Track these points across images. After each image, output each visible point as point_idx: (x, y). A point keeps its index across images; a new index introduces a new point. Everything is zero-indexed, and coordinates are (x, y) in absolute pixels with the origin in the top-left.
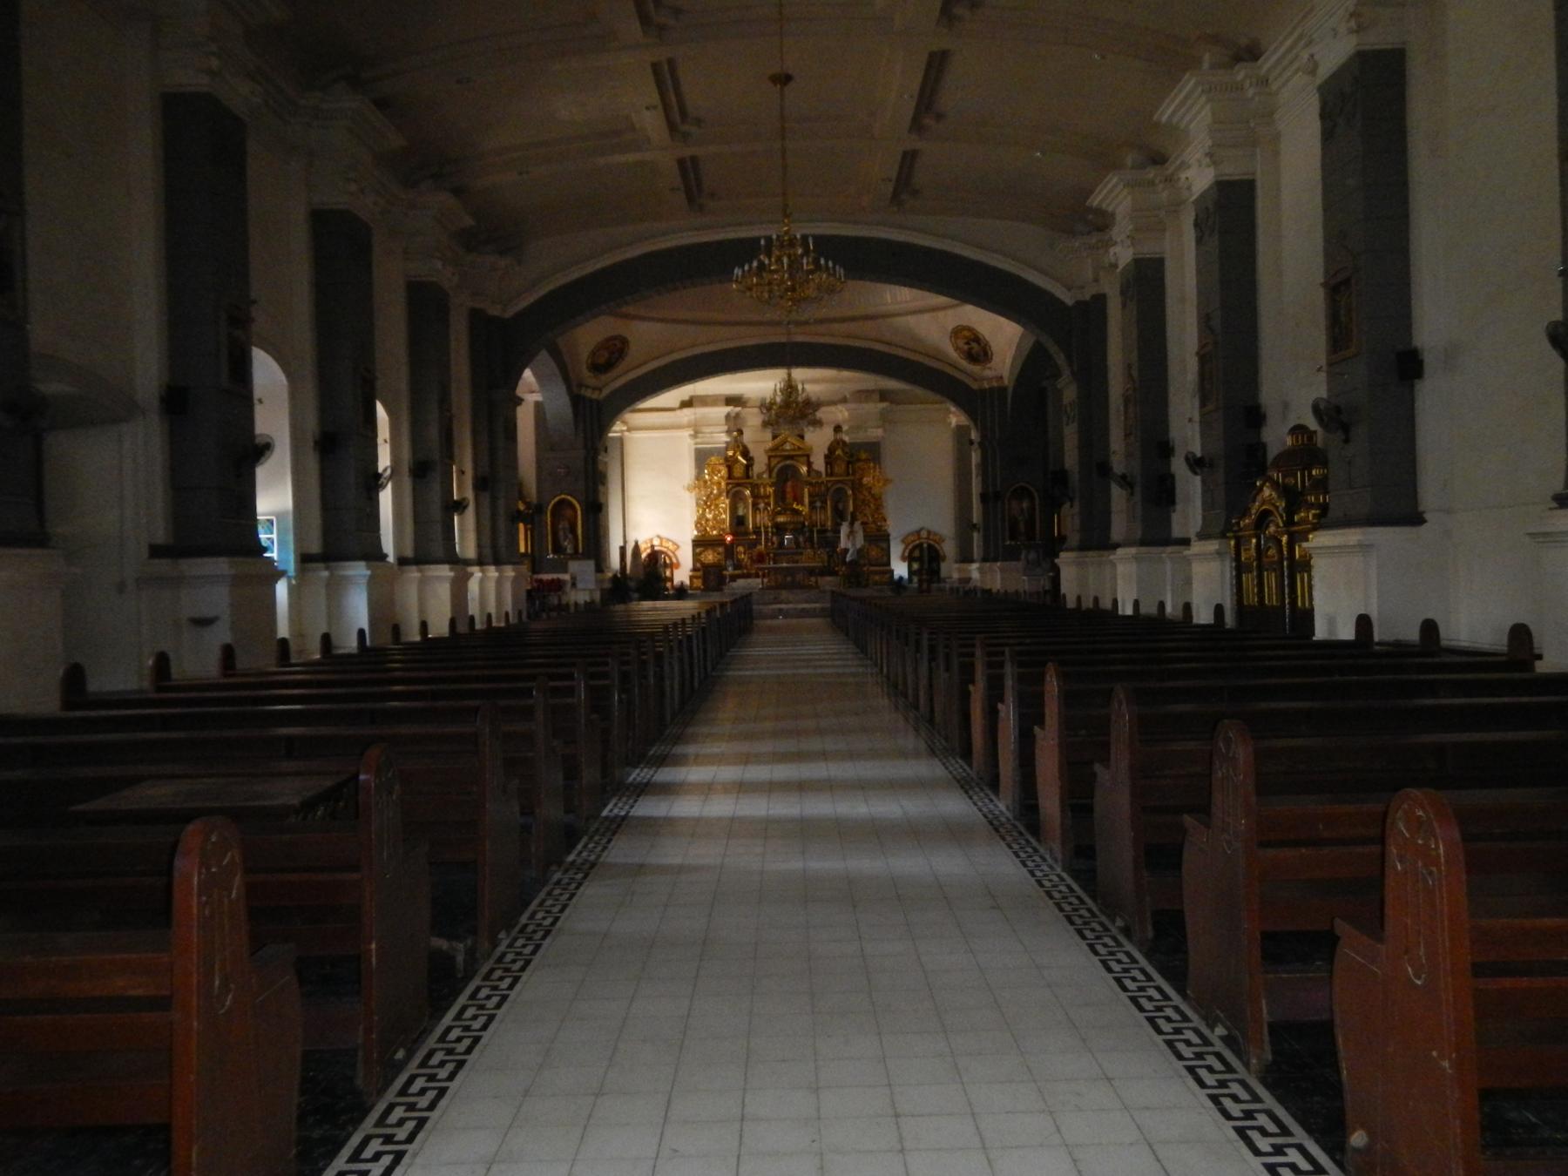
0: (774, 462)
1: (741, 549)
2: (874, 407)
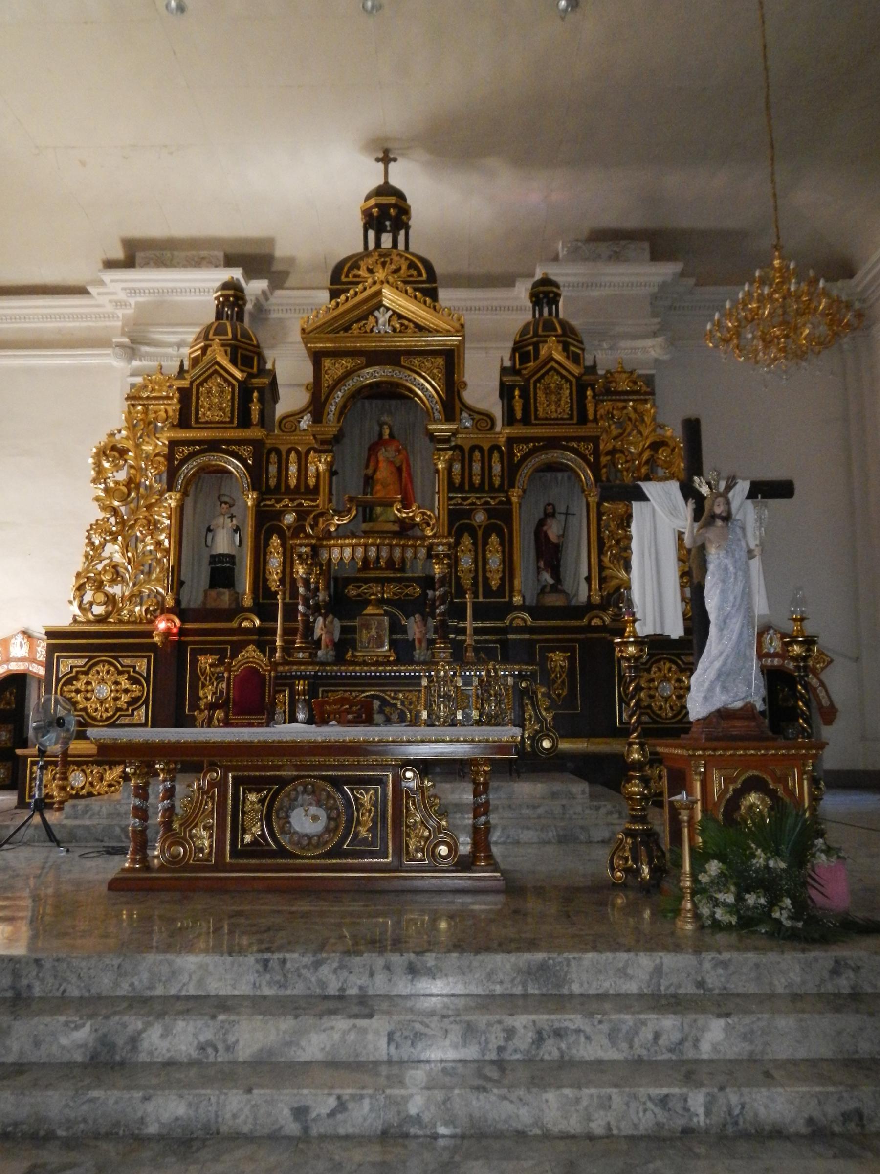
0: (333, 368)
1: (206, 661)
2: (646, 275)
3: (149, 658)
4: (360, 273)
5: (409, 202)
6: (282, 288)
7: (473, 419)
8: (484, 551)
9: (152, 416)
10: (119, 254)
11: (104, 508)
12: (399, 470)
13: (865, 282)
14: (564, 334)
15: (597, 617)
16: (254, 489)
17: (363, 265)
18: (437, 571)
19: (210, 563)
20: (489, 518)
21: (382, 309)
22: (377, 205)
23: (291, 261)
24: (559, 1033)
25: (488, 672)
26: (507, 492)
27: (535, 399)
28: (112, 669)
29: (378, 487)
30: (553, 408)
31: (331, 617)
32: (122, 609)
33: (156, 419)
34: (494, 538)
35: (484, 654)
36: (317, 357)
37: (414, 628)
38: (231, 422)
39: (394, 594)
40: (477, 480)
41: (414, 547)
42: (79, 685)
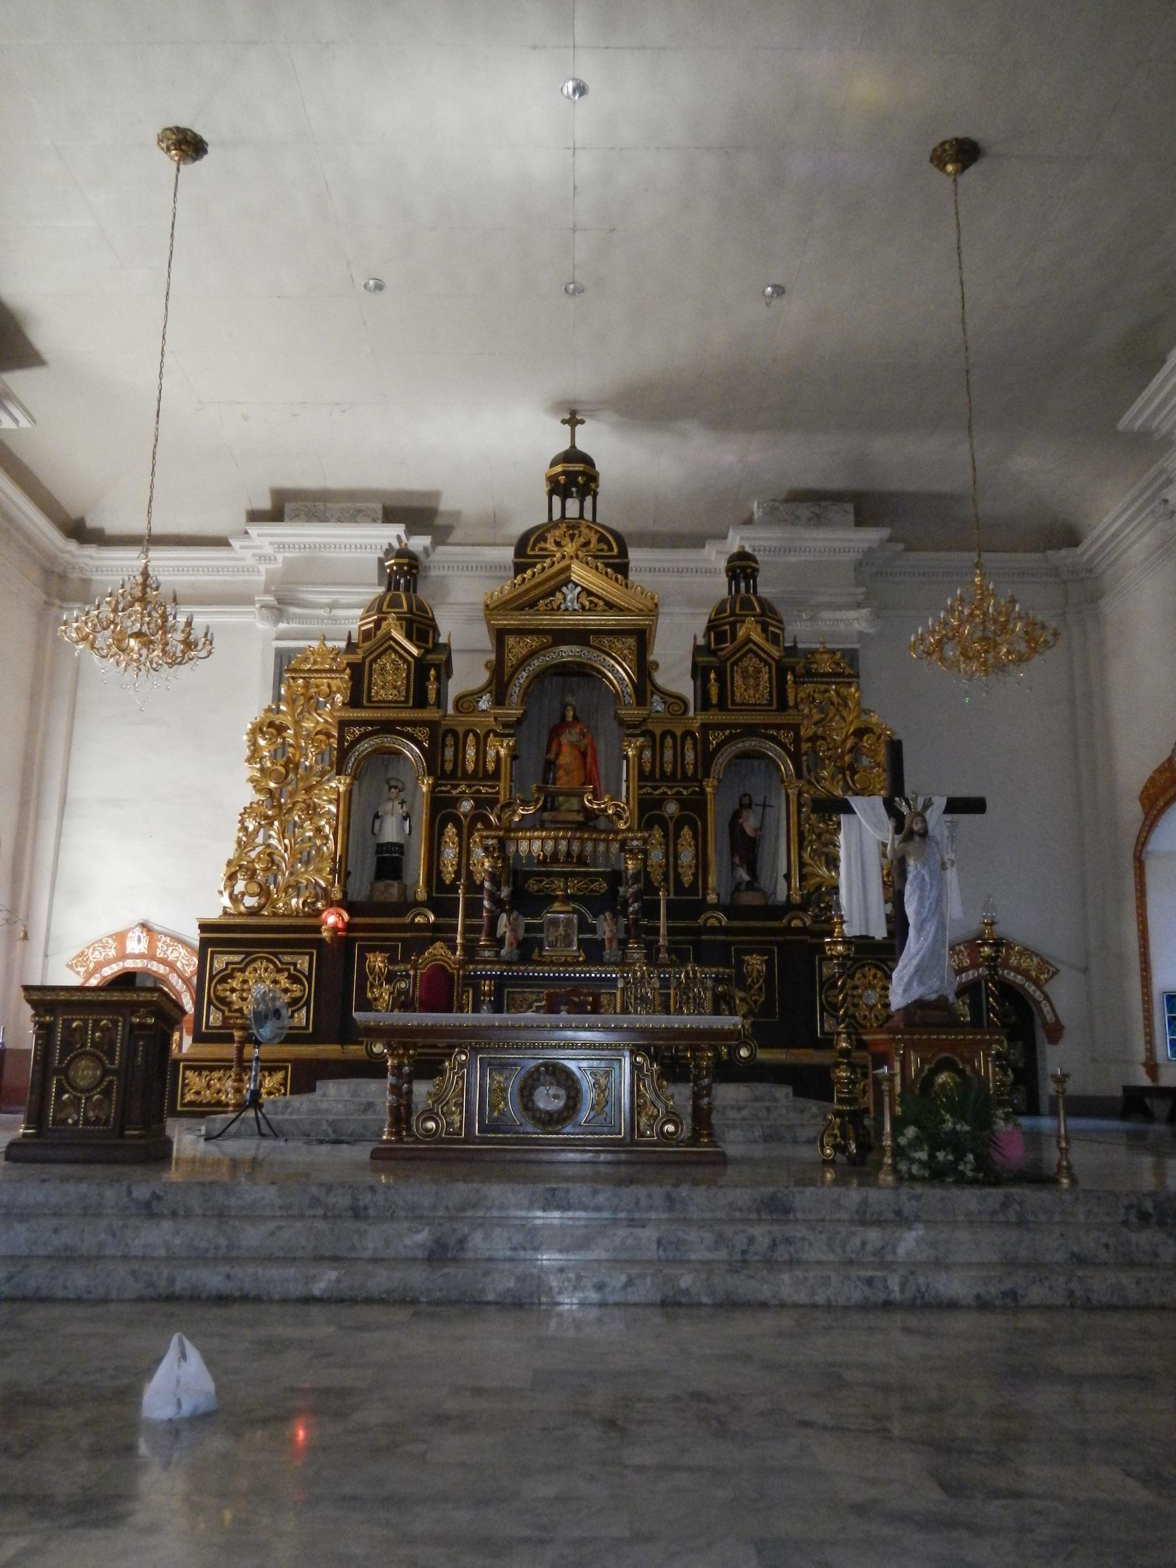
0: (517, 647)
1: (377, 961)
2: (848, 540)
3: (311, 955)
4: (548, 546)
5: (599, 467)
6: (444, 543)
7: (665, 703)
8: (676, 845)
9: (313, 690)
10: (265, 504)
11: (259, 791)
12: (584, 755)
13: (1090, 553)
14: (763, 614)
15: (797, 918)
16: (430, 774)
17: (550, 538)
18: (630, 867)
19: (377, 852)
20: (681, 810)
21: (570, 585)
22: (564, 473)
23: (457, 514)
24: (788, 1241)
25: (687, 973)
26: (701, 782)
27: (732, 684)
28: (271, 966)
29: (561, 773)
30: (751, 692)
31: (515, 913)
32: (278, 900)
33: (318, 693)
34: (686, 832)
35: (680, 956)
36: (500, 636)
37: (605, 927)
38: (406, 701)
39: (579, 889)
40: (668, 768)
41: (606, 840)
42: (235, 984)
